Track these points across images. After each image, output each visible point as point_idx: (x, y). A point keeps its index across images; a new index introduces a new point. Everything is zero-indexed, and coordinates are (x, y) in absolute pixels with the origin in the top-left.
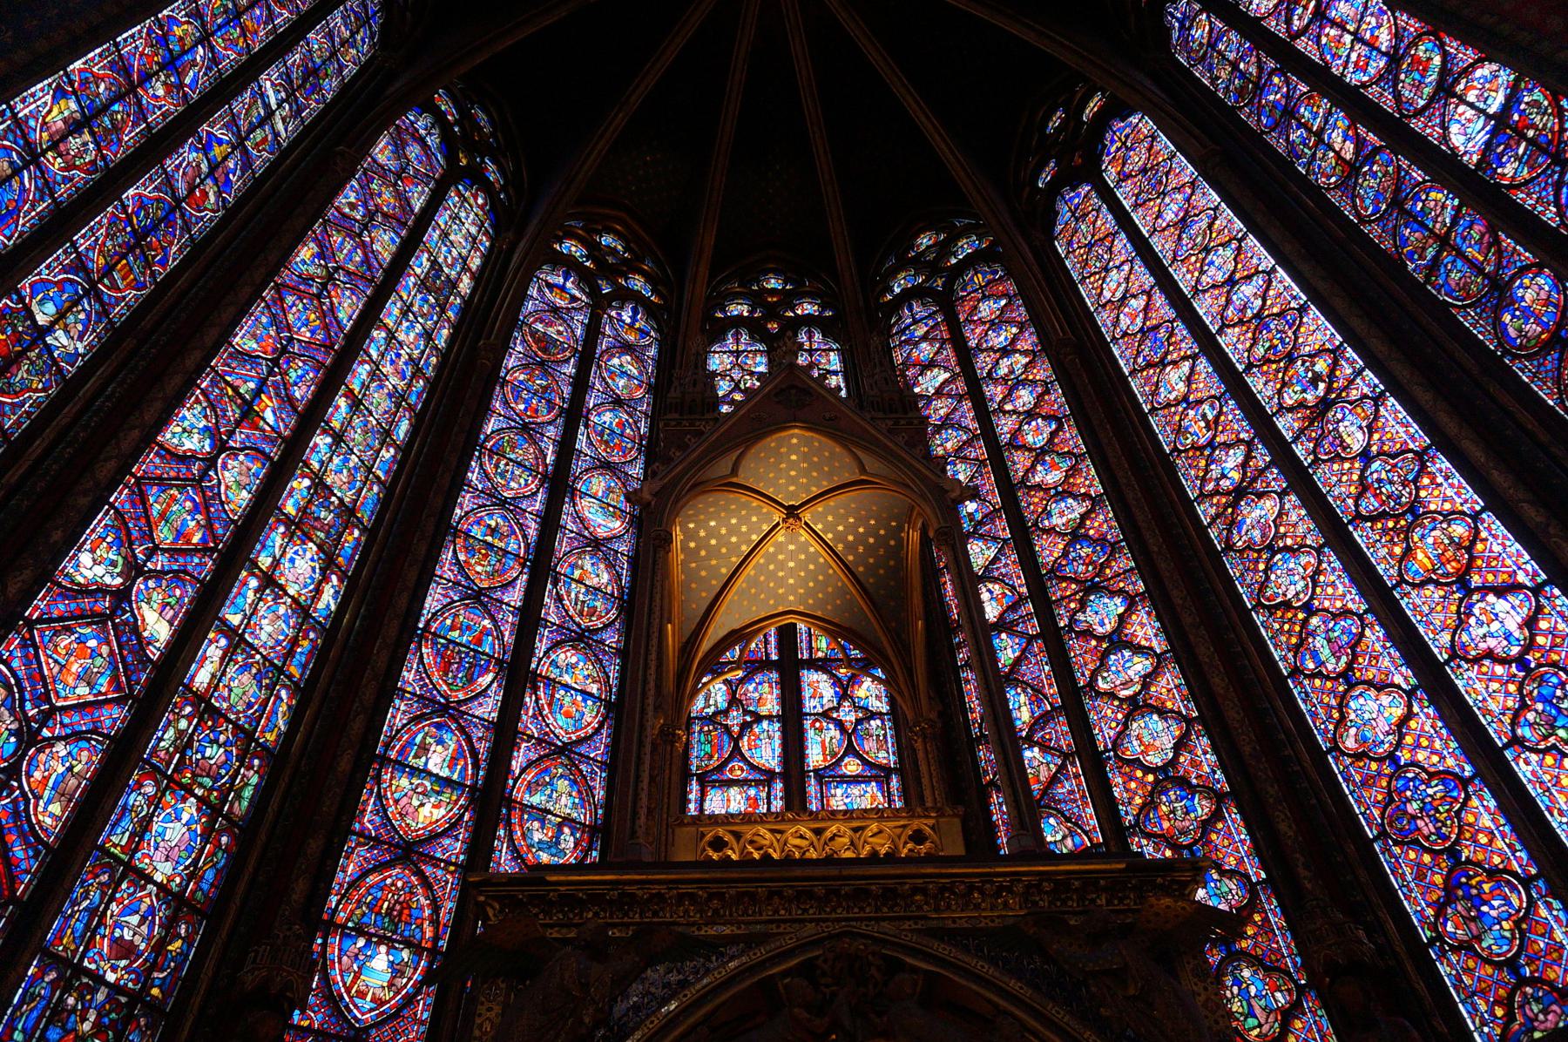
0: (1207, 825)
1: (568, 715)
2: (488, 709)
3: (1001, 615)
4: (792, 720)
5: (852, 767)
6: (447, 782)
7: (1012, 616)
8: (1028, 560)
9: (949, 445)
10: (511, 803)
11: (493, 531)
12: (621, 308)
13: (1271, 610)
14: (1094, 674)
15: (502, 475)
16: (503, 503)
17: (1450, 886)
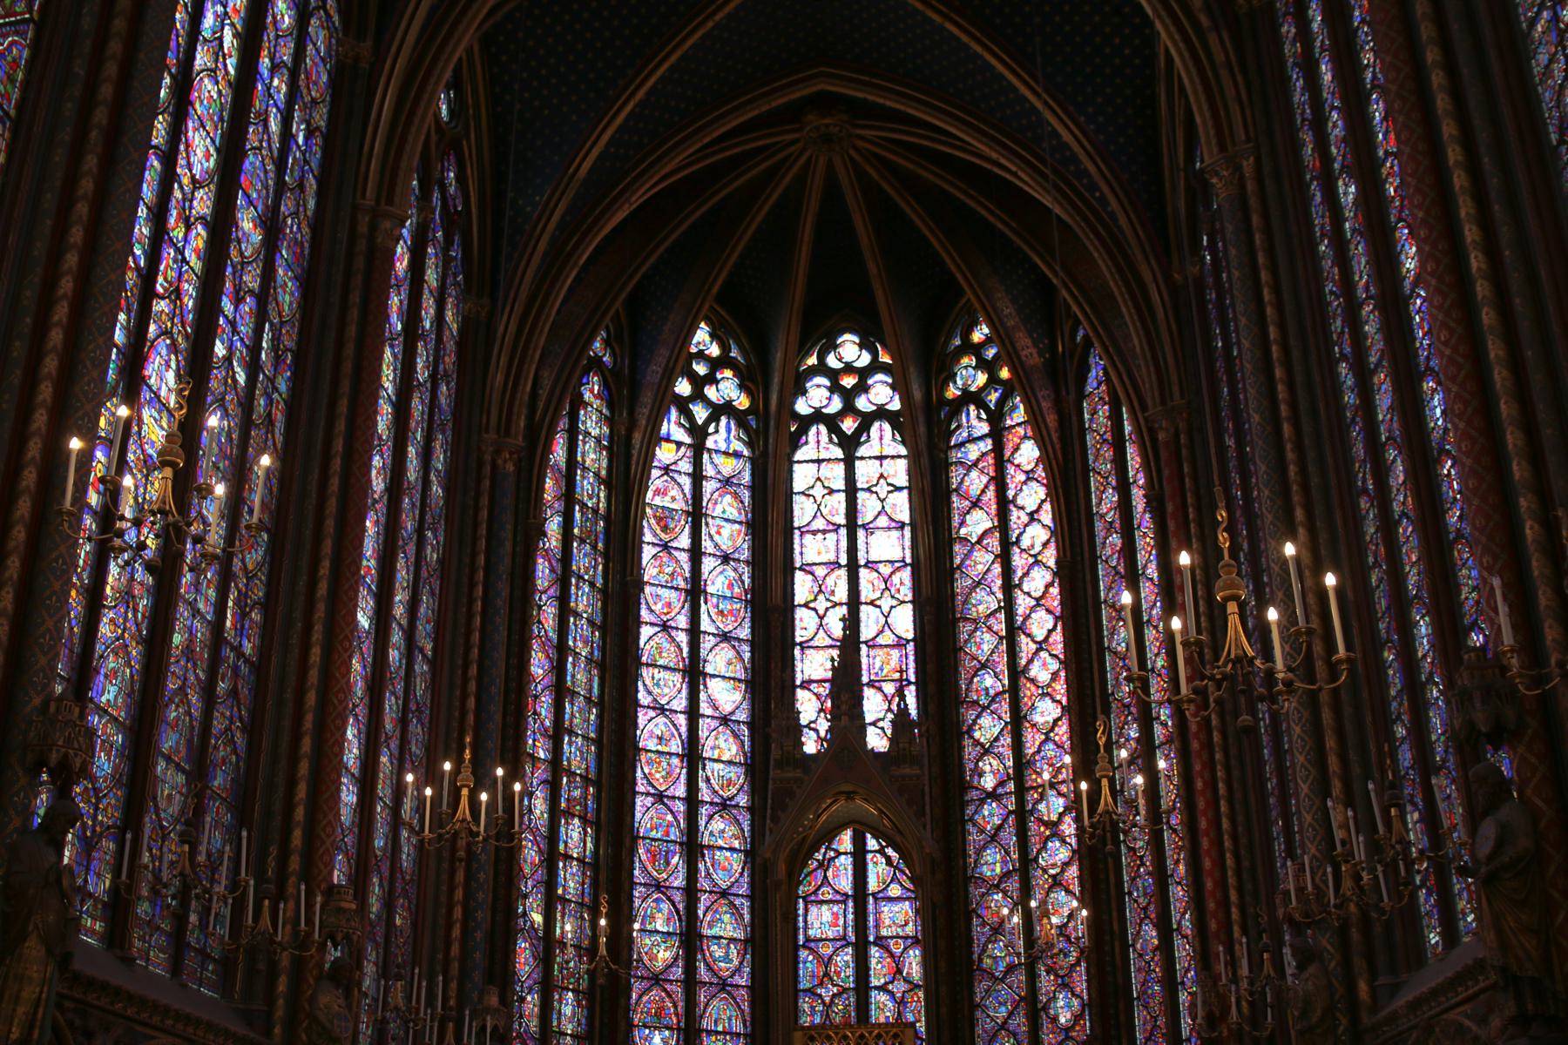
0: (1073, 966)
1: (724, 869)
2: (679, 881)
3: (995, 789)
4: (859, 855)
5: (895, 891)
6: (668, 933)
7: (1000, 790)
8: (1018, 745)
9: (981, 608)
10: (701, 936)
11: (660, 739)
12: (717, 431)
13: (1129, 849)
14: (1039, 852)
15: (658, 685)
16: (662, 710)
17: (1151, 1034)
